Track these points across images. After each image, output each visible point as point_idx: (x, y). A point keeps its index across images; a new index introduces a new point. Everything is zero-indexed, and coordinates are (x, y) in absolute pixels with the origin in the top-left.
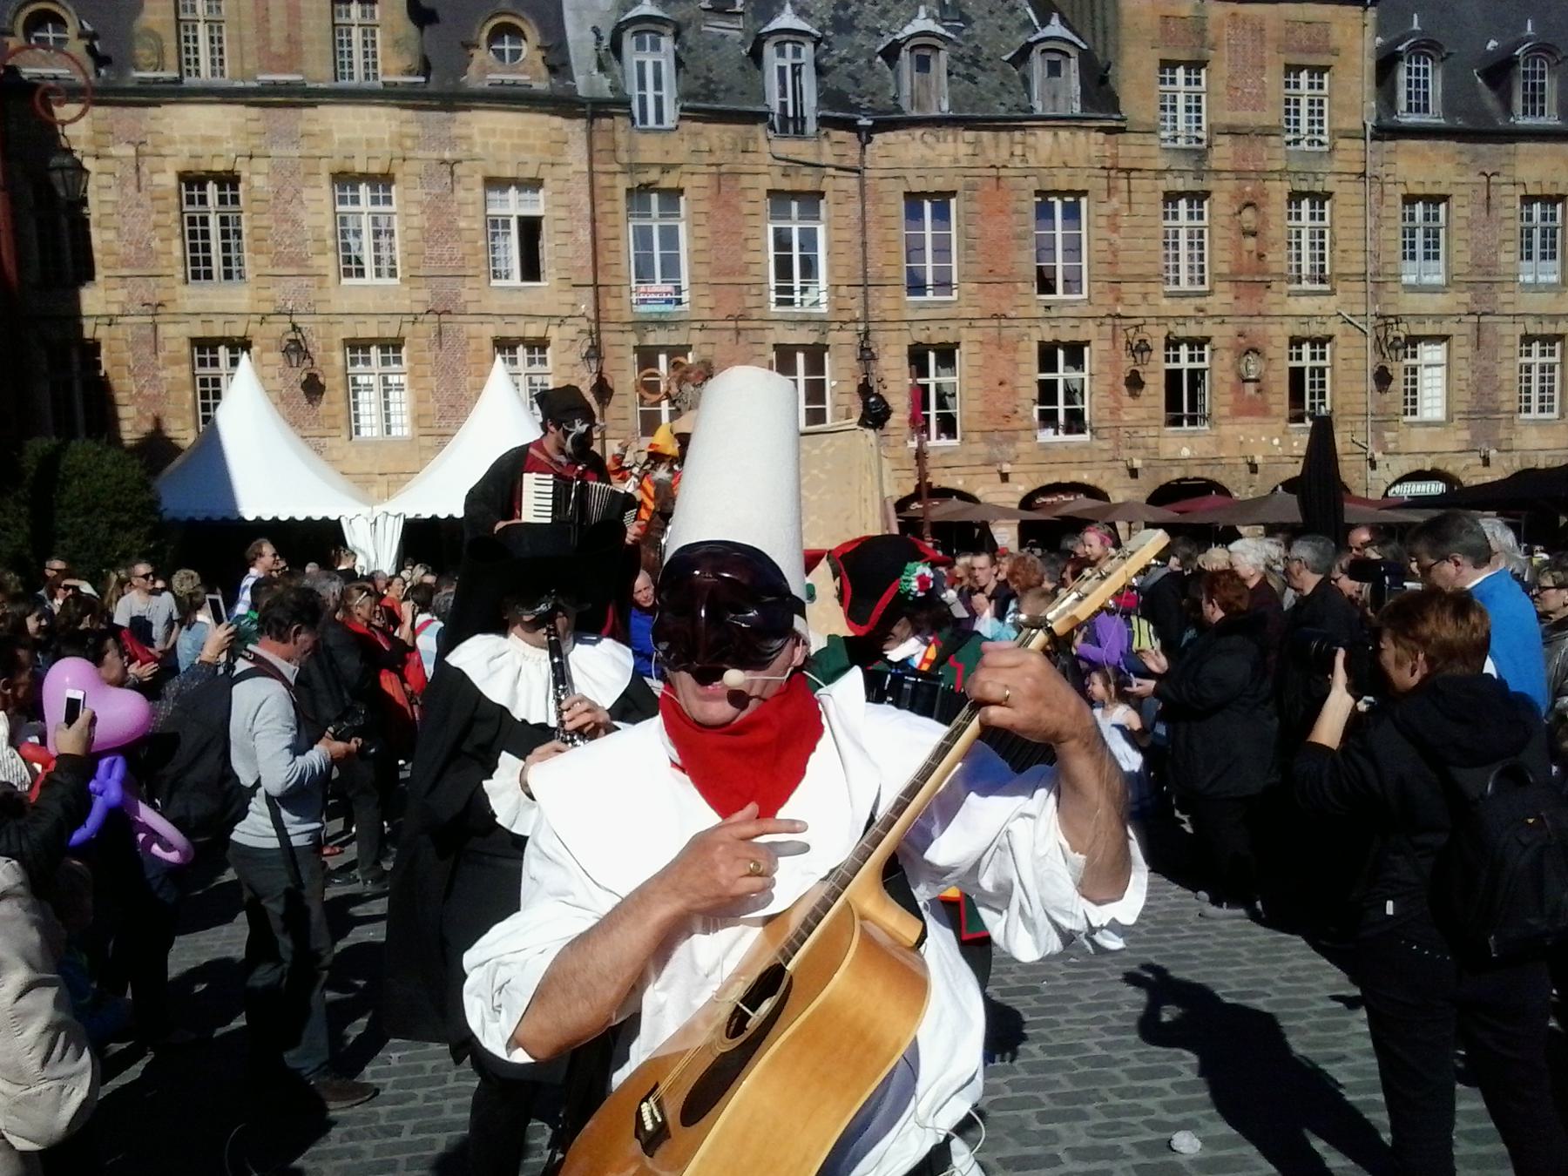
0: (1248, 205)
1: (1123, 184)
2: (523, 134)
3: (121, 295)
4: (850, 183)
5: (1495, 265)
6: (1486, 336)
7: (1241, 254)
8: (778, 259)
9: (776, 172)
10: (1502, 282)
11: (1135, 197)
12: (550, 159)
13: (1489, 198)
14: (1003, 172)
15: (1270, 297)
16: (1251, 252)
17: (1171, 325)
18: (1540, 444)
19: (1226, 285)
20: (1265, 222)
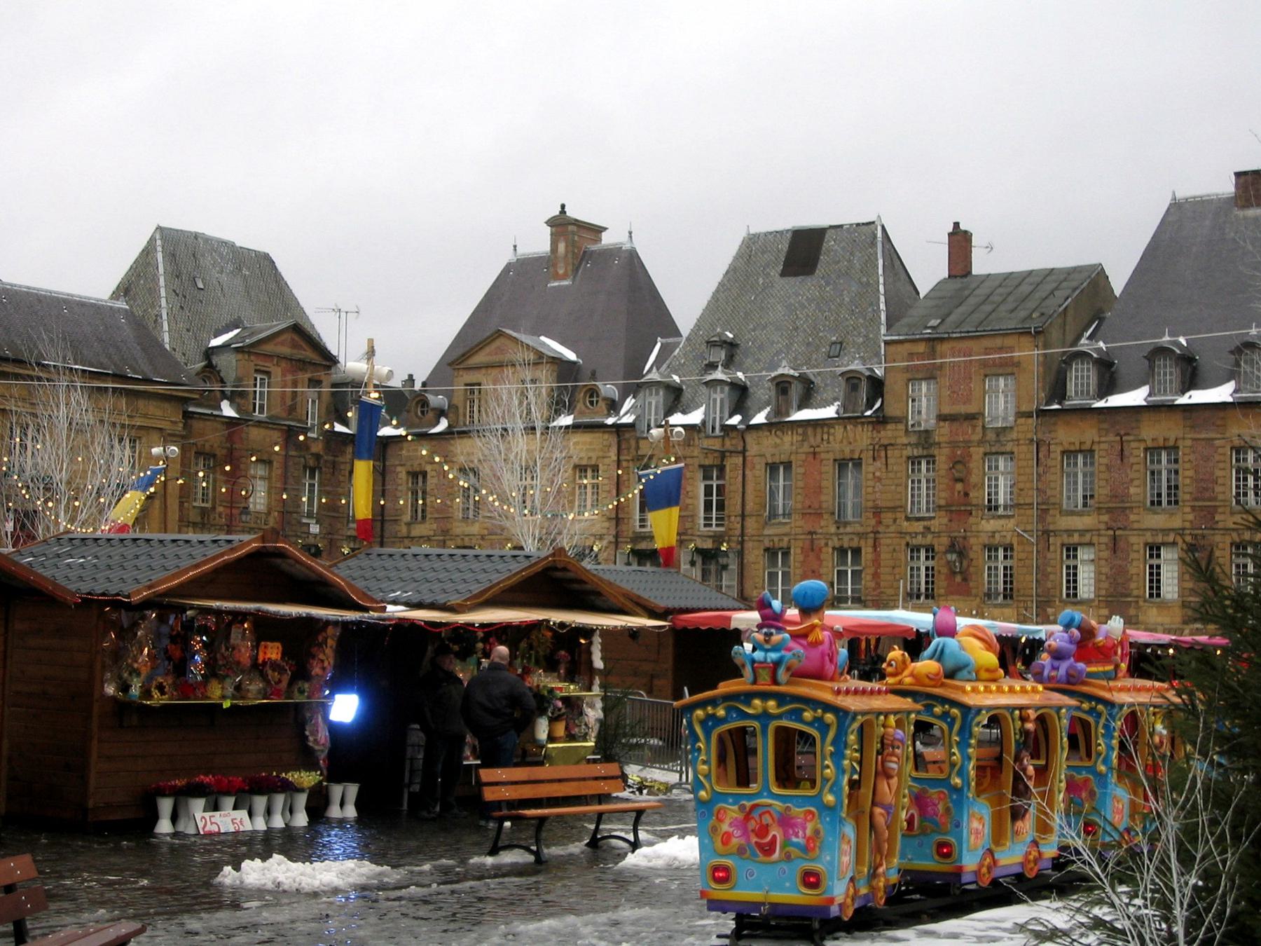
0: (959, 462)
1: (883, 454)
2: (591, 443)
3: (435, 526)
4: (739, 460)
5: (1128, 495)
6: (1121, 544)
7: (953, 494)
8: (706, 502)
9: (701, 456)
10: (1132, 508)
11: (890, 461)
12: (601, 454)
13: (1122, 450)
14: (817, 450)
15: (972, 520)
16: (959, 492)
17: (908, 538)
18: (1160, 620)
19: (943, 513)
20: (969, 472)
